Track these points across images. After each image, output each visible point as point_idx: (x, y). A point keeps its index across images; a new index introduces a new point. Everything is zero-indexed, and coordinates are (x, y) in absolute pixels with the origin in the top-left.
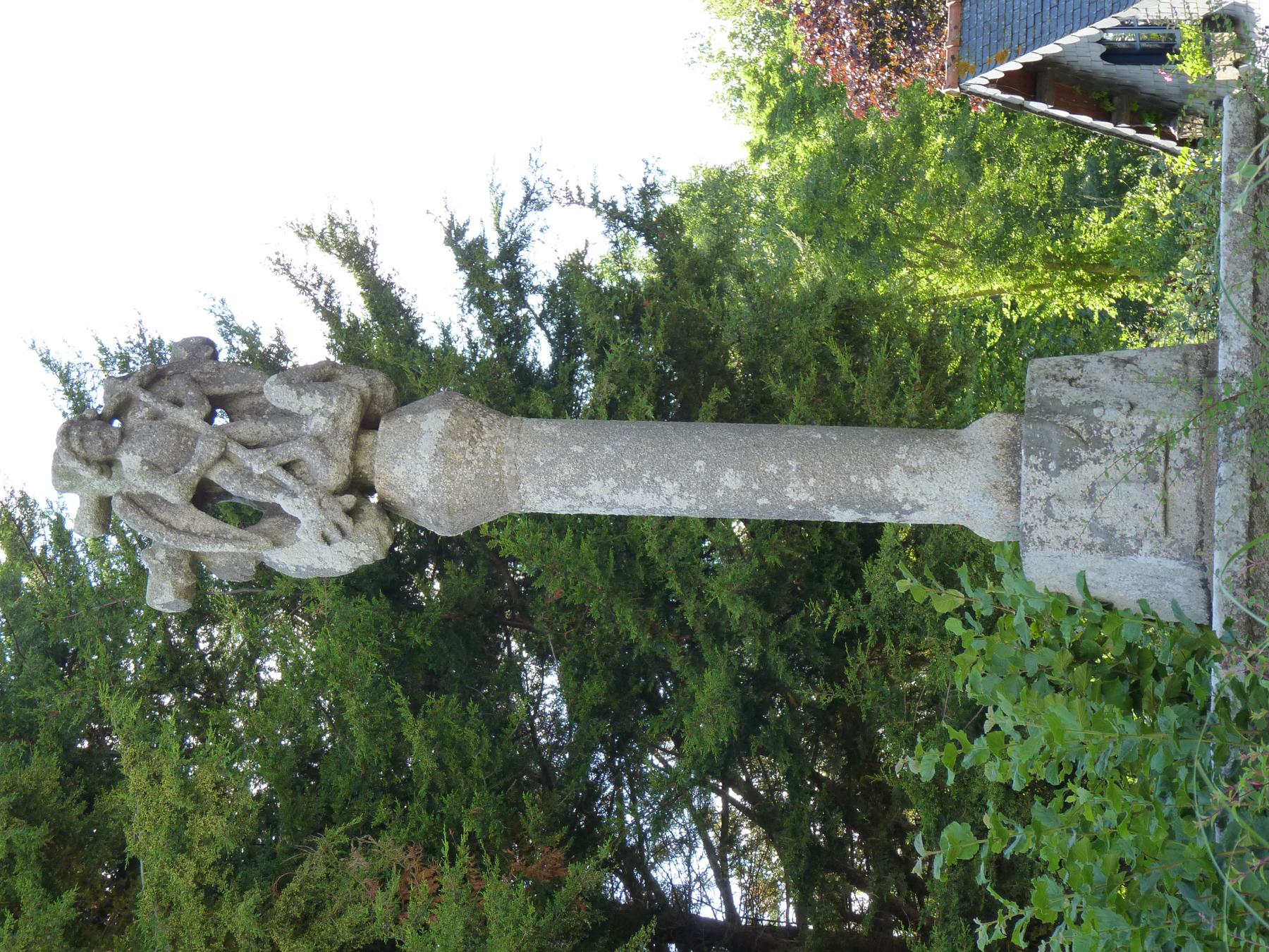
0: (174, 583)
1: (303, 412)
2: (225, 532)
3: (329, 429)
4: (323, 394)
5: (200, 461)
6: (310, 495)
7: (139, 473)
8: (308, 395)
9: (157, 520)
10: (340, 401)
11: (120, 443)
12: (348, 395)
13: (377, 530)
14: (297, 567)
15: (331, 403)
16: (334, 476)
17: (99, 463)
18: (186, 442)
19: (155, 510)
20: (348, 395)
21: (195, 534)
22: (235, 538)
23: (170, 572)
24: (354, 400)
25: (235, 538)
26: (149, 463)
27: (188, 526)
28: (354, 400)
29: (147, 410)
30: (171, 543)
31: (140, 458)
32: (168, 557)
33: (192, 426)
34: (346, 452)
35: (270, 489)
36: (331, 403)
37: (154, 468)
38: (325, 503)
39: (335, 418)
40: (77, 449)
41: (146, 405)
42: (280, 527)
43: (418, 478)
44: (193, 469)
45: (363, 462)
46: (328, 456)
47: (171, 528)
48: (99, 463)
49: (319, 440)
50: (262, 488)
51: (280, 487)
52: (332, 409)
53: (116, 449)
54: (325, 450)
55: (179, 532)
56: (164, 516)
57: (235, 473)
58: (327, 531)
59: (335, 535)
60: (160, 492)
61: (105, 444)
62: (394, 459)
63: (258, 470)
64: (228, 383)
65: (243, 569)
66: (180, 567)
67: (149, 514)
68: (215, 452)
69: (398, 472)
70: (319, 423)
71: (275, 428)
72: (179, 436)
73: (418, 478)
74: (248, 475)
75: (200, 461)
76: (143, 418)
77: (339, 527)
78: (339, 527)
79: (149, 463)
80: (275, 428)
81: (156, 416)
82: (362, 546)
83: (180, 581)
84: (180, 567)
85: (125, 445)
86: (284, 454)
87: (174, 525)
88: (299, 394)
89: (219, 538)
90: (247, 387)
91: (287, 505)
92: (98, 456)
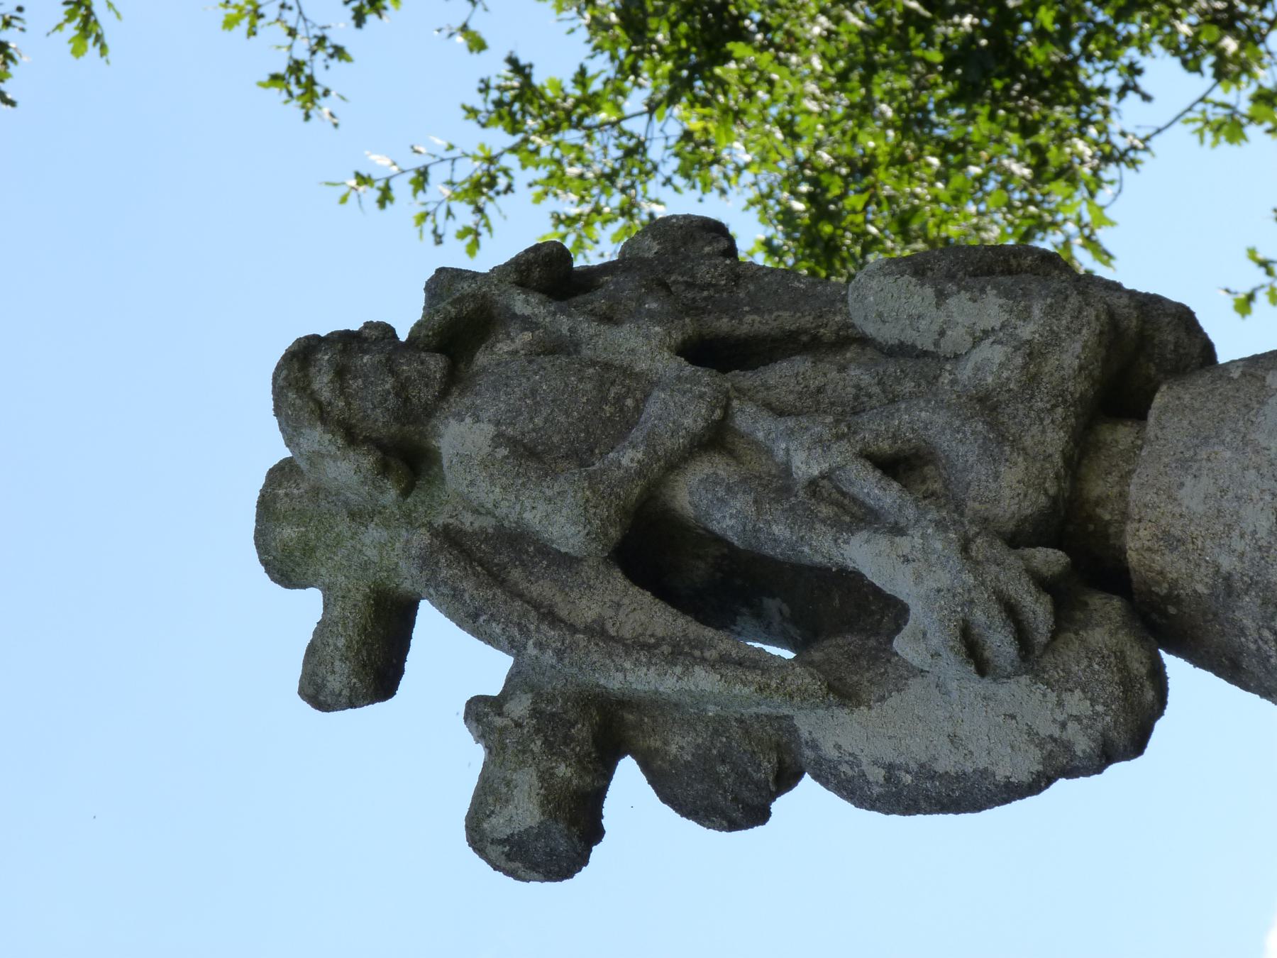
0: (546, 777)
1: (947, 347)
2: (699, 644)
3: (1012, 376)
4: (1007, 293)
5: (651, 441)
6: (940, 525)
7: (484, 465)
8: (964, 295)
9: (521, 596)
10: (1050, 311)
11: (444, 394)
12: (1074, 300)
13: (1121, 657)
14: (890, 767)
15: (1026, 315)
16: (1010, 489)
17: (377, 444)
18: (619, 399)
19: (516, 574)
20: (1074, 300)
21: (619, 640)
22: (725, 660)
23: (537, 746)
24: (1090, 313)
25: (725, 660)
26: (513, 442)
27: (601, 621)
28: (1090, 313)
29: (527, 336)
30: (549, 658)
31: (490, 429)
32: (535, 712)
33: (642, 366)
34: (1055, 440)
35: (836, 524)
36: (1026, 315)
37: (528, 454)
38: (980, 547)
39: (1033, 353)
40: (325, 395)
41: (528, 323)
42: (854, 658)
43: (1247, 511)
44: (630, 457)
45: (1098, 486)
46: (1001, 439)
47: (550, 616)
48: (377, 444)
49: (986, 404)
50: (811, 519)
51: (864, 518)
52: (1027, 331)
53: (429, 412)
54: (992, 425)
55: (573, 629)
56: (542, 589)
57: (744, 480)
58: (979, 616)
59: (1000, 644)
60: (533, 518)
61: (402, 388)
62: (1184, 464)
63: (806, 465)
64: (756, 310)
65: (743, 776)
66: (568, 740)
67: (496, 578)
68: (694, 419)
69: (1194, 496)
70: (991, 363)
71: (866, 379)
72: (601, 385)
73: (1247, 511)
74: (778, 486)
75: (651, 441)
76: (515, 352)
77: (1011, 611)
78: (1011, 611)
79: (513, 442)
80: (866, 379)
81: (556, 347)
82: (1076, 703)
83: (563, 770)
84: (568, 740)
85: (457, 402)
86: (877, 431)
87: (563, 613)
88: (941, 296)
89: (679, 653)
90: (807, 321)
91: (866, 555)
92: (380, 421)
